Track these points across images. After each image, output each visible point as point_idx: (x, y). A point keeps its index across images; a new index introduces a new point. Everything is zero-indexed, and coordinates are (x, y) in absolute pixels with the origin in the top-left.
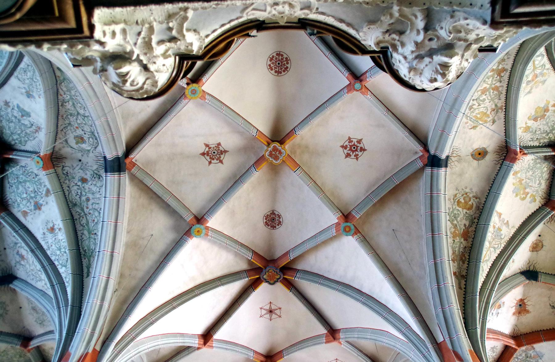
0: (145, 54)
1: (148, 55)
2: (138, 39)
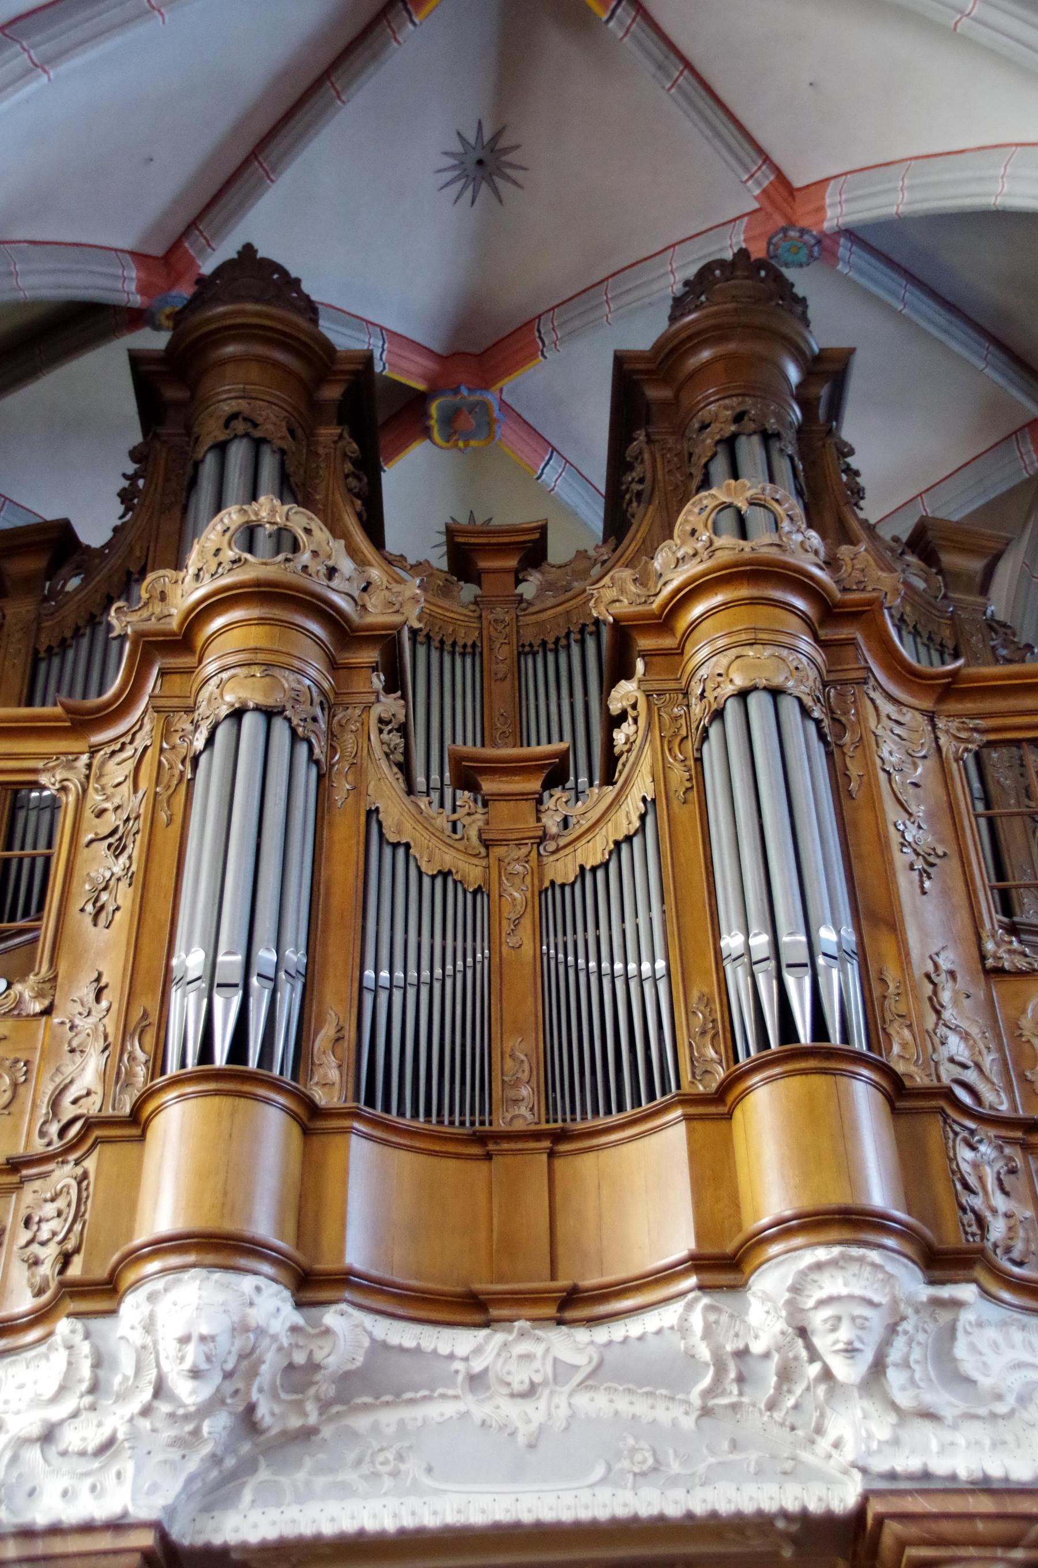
0: (796, 1358)
1: (791, 1355)
2: (801, 1396)
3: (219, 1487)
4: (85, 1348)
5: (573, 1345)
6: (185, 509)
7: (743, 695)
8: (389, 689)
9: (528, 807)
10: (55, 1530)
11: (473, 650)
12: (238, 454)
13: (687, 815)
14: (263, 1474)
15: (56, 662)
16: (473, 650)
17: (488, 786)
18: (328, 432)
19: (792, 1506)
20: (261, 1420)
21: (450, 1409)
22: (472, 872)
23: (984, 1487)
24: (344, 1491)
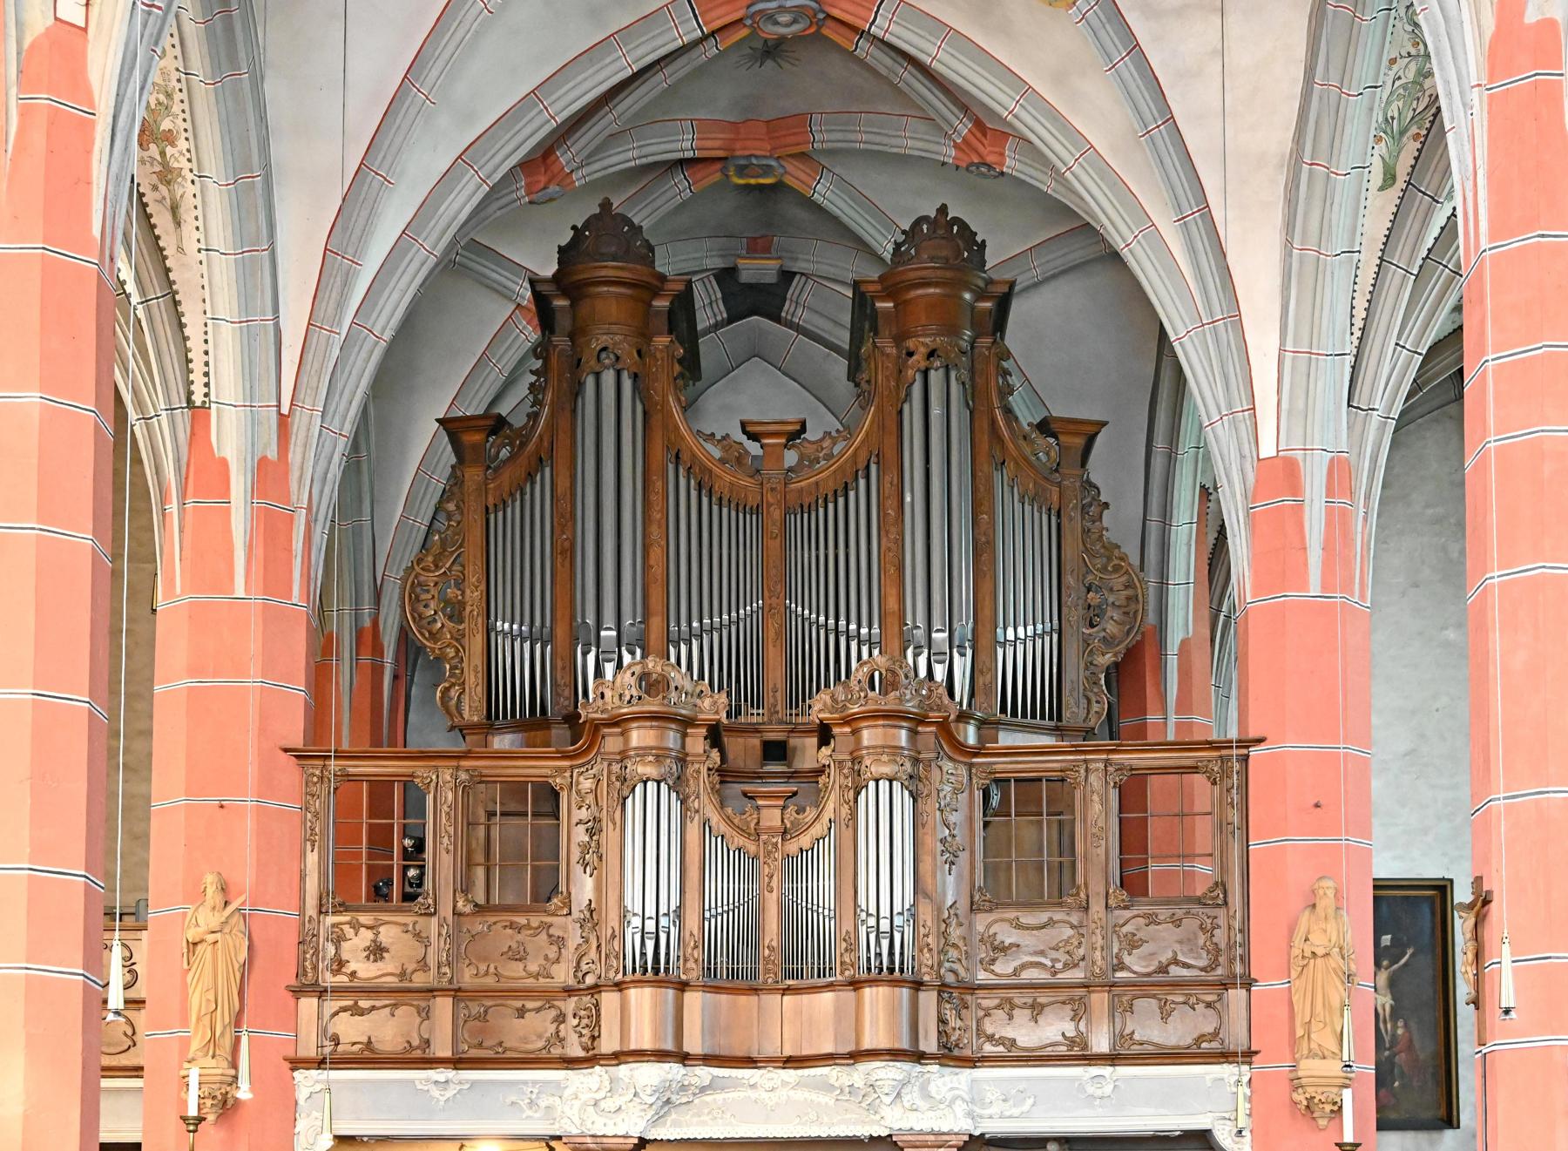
3: (657, 1120)
4: (606, 1077)
6: (574, 411)
8: (712, 746)
9: (778, 812)
11: (757, 510)
12: (608, 378)
13: (848, 833)
14: (674, 1116)
15: (500, 514)
16: (757, 510)
18: (662, 341)
21: (742, 1094)
22: (752, 848)
23: (932, 1133)
24: (704, 1123)
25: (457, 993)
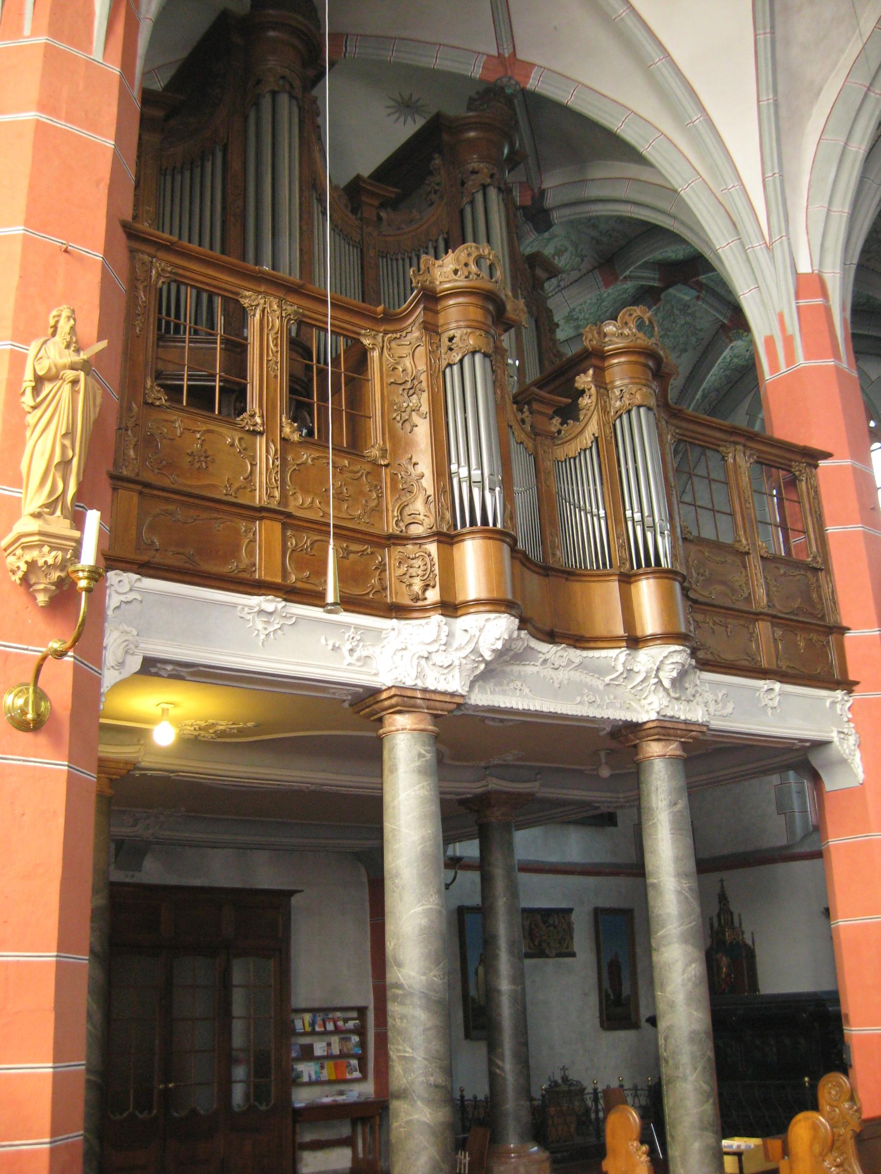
5: (576, 655)
7: (639, 407)
10: (435, 692)
17: (535, 406)
19: (623, 718)
20: (497, 667)
21: (535, 669)
24: (504, 692)
25: (288, 520)
